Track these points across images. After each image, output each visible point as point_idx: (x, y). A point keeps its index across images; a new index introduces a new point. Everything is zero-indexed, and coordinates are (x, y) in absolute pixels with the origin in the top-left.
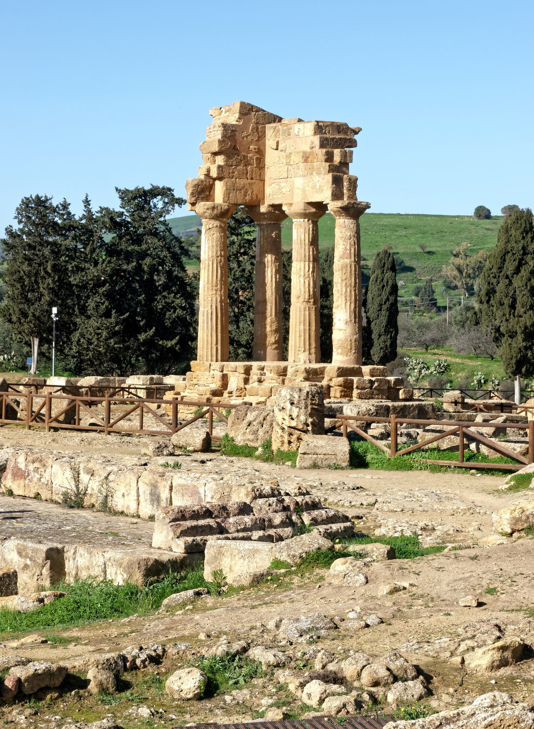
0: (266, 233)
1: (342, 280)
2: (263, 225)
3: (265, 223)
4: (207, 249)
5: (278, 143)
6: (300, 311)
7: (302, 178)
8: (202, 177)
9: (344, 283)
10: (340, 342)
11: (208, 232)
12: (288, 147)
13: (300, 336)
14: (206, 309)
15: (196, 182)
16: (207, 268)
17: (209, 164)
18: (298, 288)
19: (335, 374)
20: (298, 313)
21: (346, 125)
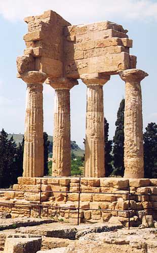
0: (62, 95)
1: (133, 122)
2: (61, 90)
3: (62, 89)
4: (31, 102)
5: (75, 37)
6: (95, 144)
8: (28, 56)
9: (135, 123)
10: (133, 163)
12: (83, 39)
13: (95, 160)
14: (31, 143)
15: (24, 58)
16: (31, 115)
17: (31, 48)
18: (93, 128)
20: (93, 144)
21: (121, 26)
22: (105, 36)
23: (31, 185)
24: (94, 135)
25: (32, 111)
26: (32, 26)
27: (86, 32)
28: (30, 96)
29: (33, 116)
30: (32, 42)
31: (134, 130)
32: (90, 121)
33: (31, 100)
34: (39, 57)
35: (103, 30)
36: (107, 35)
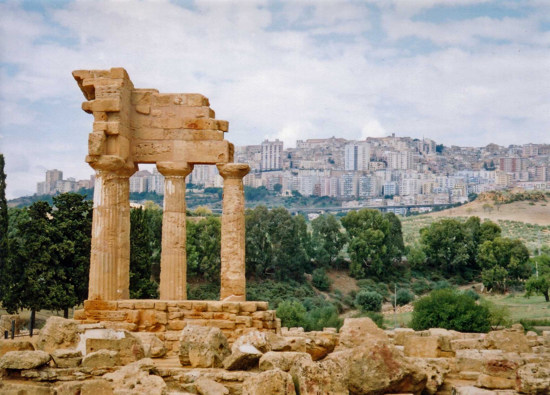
1: (238, 230)
2: (122, 178)
7: (184, 142)
10: (236, 282)
11: (107, 183)
16: (107, 215)
19: (255, 309)
22: (198, 115)
23: (109, 311)
24: (177, 243)
25: (107, 210)
26: (105, 91)
27: (168, 105)
28: (105, 188)
29: (109, 217)
30: (103, 114)
31: (238, 240)
32: (173, 224)
33: (107, 194)
34: (116, 136)
35: (197, 106)
36: (202, 114)
